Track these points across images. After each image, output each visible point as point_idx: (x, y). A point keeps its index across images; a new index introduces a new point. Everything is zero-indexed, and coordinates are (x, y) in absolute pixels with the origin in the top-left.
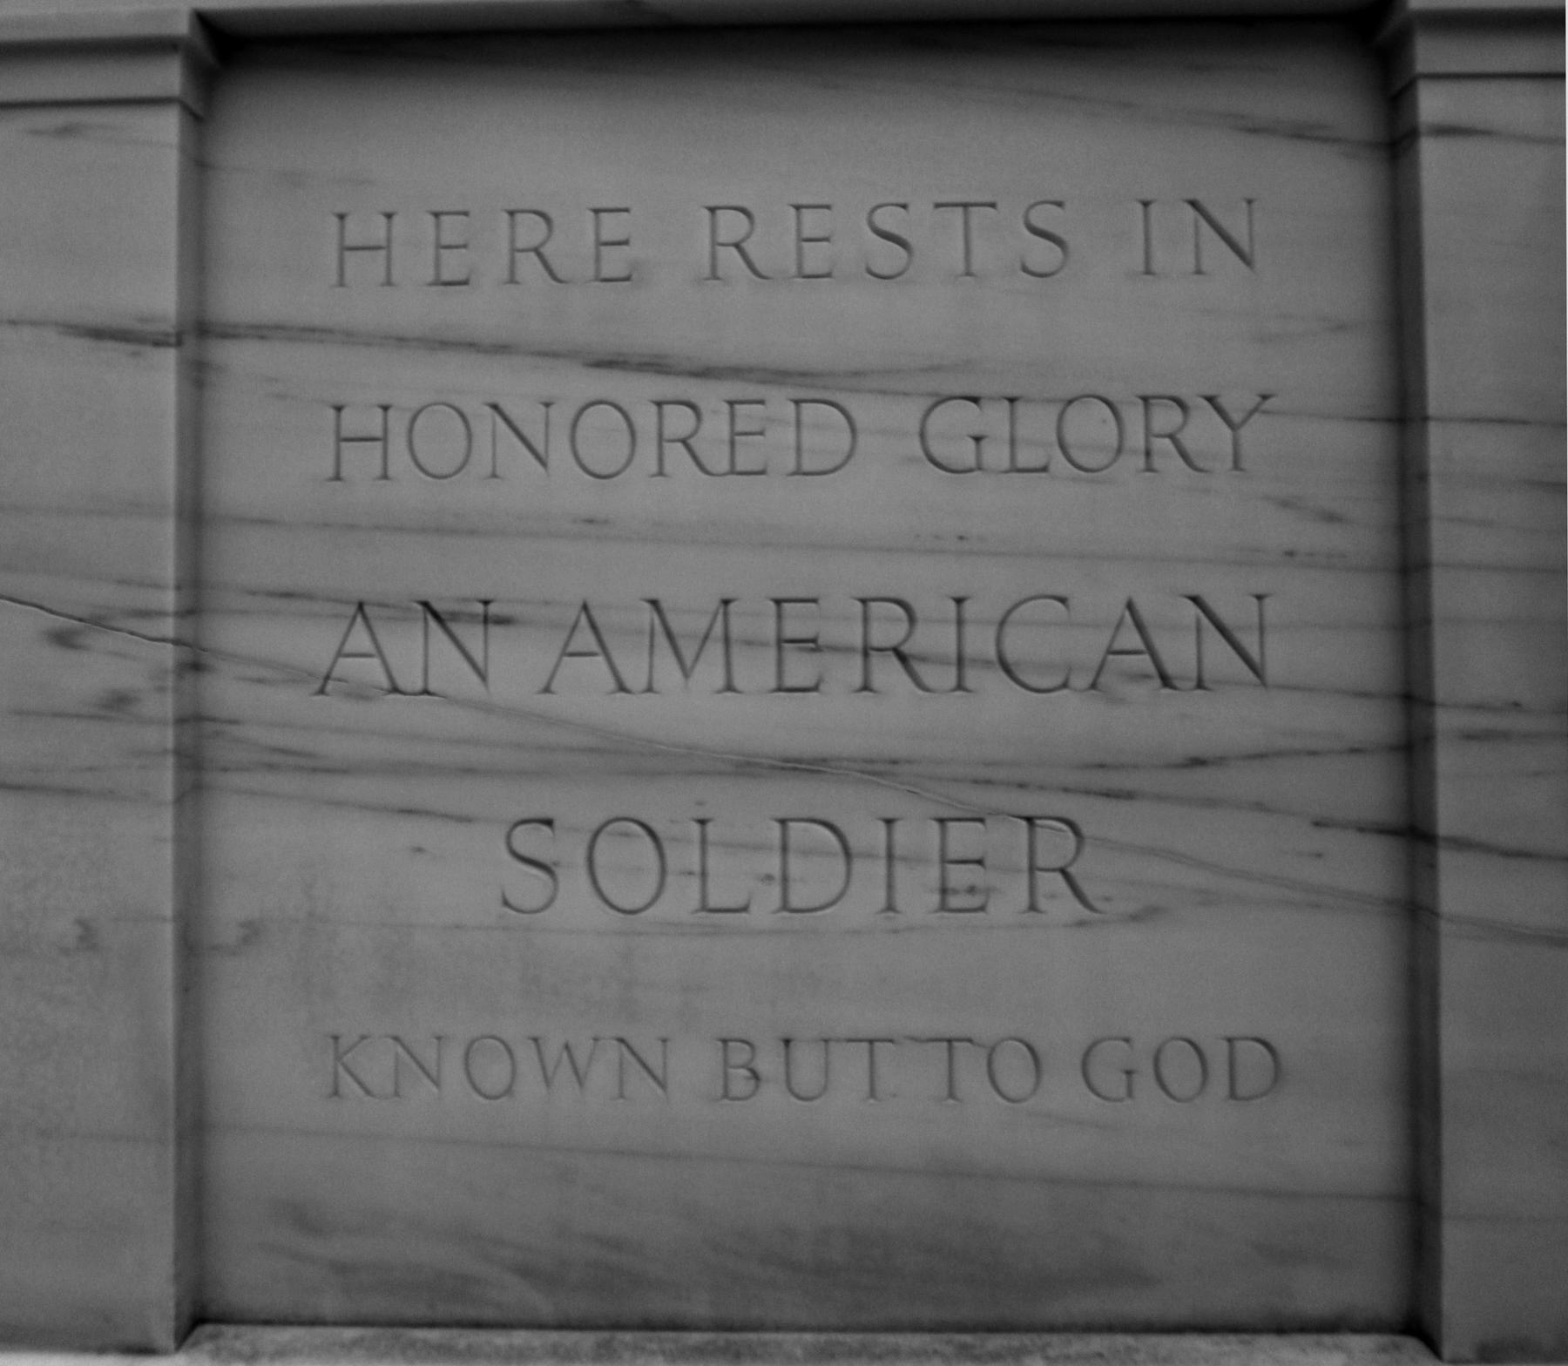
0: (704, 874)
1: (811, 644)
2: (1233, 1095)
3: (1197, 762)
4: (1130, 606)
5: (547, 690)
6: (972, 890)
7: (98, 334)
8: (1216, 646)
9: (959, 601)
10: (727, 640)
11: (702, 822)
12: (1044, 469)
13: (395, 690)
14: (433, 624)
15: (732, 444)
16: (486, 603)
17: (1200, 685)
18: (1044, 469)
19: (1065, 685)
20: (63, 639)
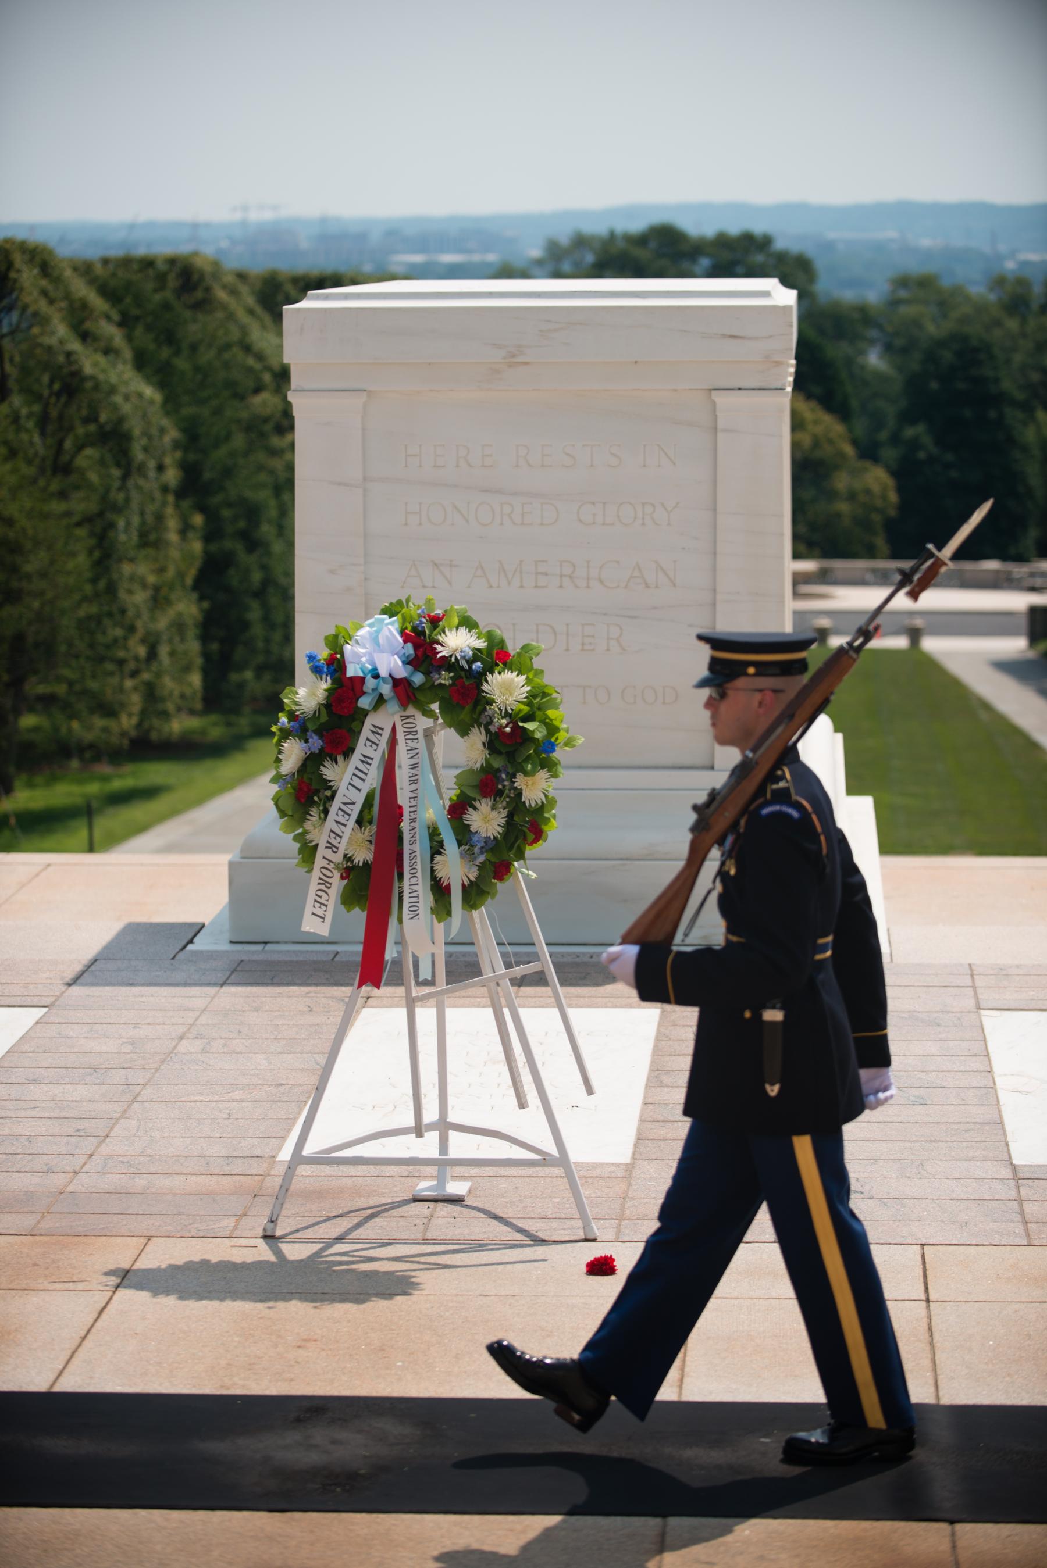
0: (514, 639)
1: (546, 574)
2: (664, 703)
3: (655, 608)
5: (469, 587)
6: (590, 644)
7: (340, 484)
9: (588, 562)
10: (521, 572)
11: (514, 625)
13: (424, 587)
15: (523, 515)
16: (451, 561)
17: (657, 587)
19: (618, 587)
20: (332, 572)
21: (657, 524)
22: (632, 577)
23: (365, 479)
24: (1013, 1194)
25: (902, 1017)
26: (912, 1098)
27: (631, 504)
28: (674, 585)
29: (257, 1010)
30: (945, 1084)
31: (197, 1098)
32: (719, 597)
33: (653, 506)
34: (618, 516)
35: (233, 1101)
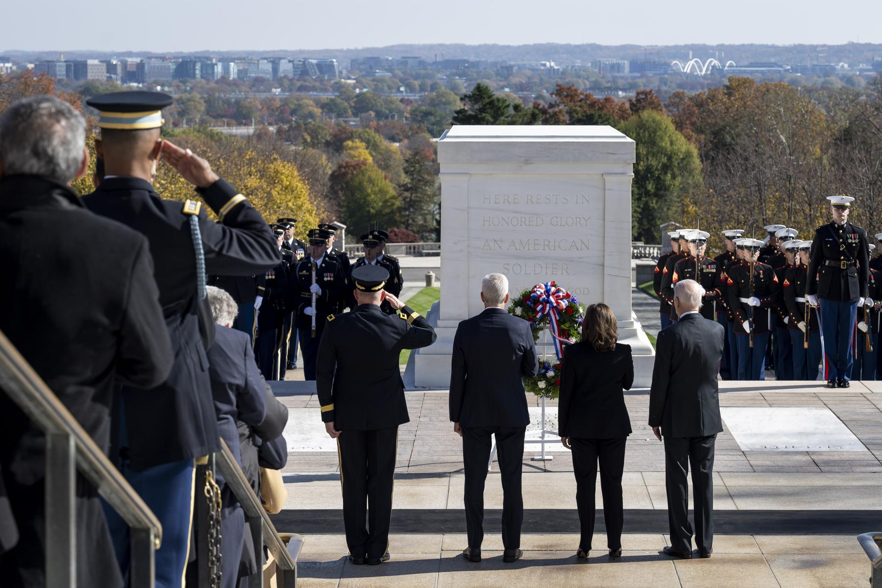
1: (538, 244)
4: (574, 241)
20: (455, 243)
24: (745, 458)
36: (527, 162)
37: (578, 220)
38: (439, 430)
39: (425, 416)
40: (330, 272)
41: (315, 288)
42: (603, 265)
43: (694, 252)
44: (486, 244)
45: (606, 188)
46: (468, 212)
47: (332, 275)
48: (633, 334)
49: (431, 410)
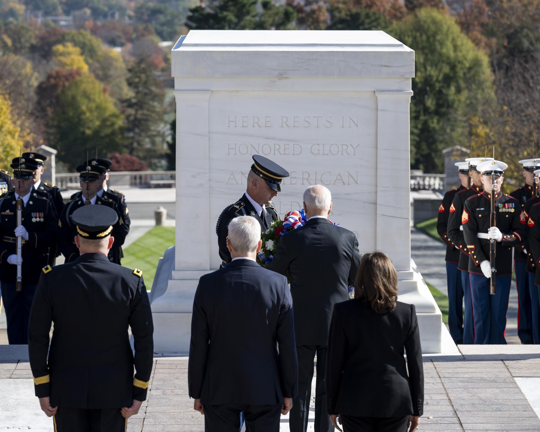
1: (296, 178)
3: (348, 194)
8: (351, 179)
11: (280, 202)
12: (328, 154)
13: (237, 184)
14: (242, 174)
15: (284, 150)
17: (348, 184)
18: (328, 154)
19: (330, 184)
20: (194, 176)
21: (349, 154)
22: (337, 179)
23: (209, 132)
25: (478, 380)
26: (494, 409)
27: (337, 145)
28: (357, 183)
29: (177, 378)
30: (506, 404)
31: (174, 411)
32: (379, 189)
33: (347, 146)
34: (330, 151)
35: (191, 412)
36: (281, 76)
37: (345, 147)
38: (174, 405)
39: (157, 389)
40: (39, 212)
41: (20, 231)
42: (376, 204)
43: (488, 187)
44: (232, 177)
45: (379, 108)
46: (209, 138)
47: (42, 214)
48: (412, 288)
49: (164, 380)
